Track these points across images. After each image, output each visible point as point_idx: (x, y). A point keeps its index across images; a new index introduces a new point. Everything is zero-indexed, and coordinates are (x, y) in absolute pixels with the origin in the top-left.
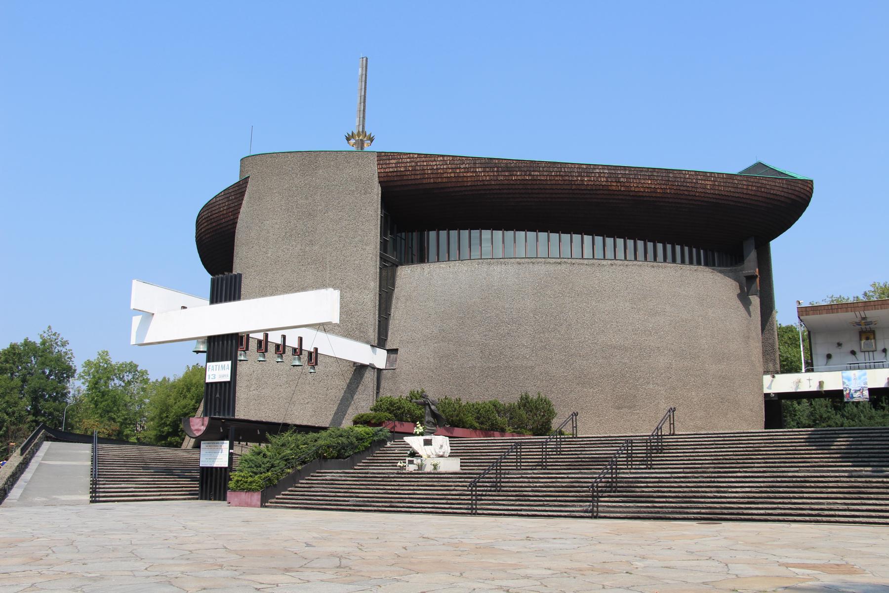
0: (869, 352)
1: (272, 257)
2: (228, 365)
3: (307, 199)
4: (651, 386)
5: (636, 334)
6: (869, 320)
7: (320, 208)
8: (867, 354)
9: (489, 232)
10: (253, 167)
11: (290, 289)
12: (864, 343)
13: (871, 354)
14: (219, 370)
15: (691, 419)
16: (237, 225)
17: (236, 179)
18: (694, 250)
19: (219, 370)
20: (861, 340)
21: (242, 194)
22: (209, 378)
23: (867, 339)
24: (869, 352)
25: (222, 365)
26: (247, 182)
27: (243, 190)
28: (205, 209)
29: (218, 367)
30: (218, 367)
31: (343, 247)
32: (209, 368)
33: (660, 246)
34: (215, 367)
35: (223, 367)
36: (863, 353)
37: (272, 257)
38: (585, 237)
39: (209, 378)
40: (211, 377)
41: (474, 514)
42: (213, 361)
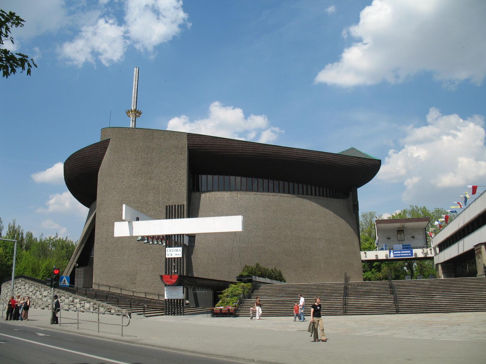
0: (401, 241)
1: (126, 184)
2: (180, 249)
3: (147, 154)
4: (317, 257)
5: (310, 232)
6: (405, 226)
7: (155, 160)
8: (400, 241)
9: (240, 177)
10: (112, 134)
11: (138, 202)
12: (399, 236)
13: (402, 241)
14: (174, 251)
15: (335, 273)
16: (102, 165)
17: (97, 139)
18: (325, 189)
19: (174, 251)
20: (398, 234)
21: (106, 148)
22: (168, 255)
23: (400, 234)
24: (401, 241)
25: (176, 250)
26: (109, 142)
27: (105, 146)
28: (79, 153)
29: (173, 250)
30: (173, 250)
31: (169, 182)
32: (167, 251)
33: (309, 187)
34: (171, 250)
35: (177, 251)
36: (398, 241)
37: (126, 184)
38: (280, 182)
39: (168, 255)
40: (169, 255)
41: (345, 315)
42: (170, 247)
